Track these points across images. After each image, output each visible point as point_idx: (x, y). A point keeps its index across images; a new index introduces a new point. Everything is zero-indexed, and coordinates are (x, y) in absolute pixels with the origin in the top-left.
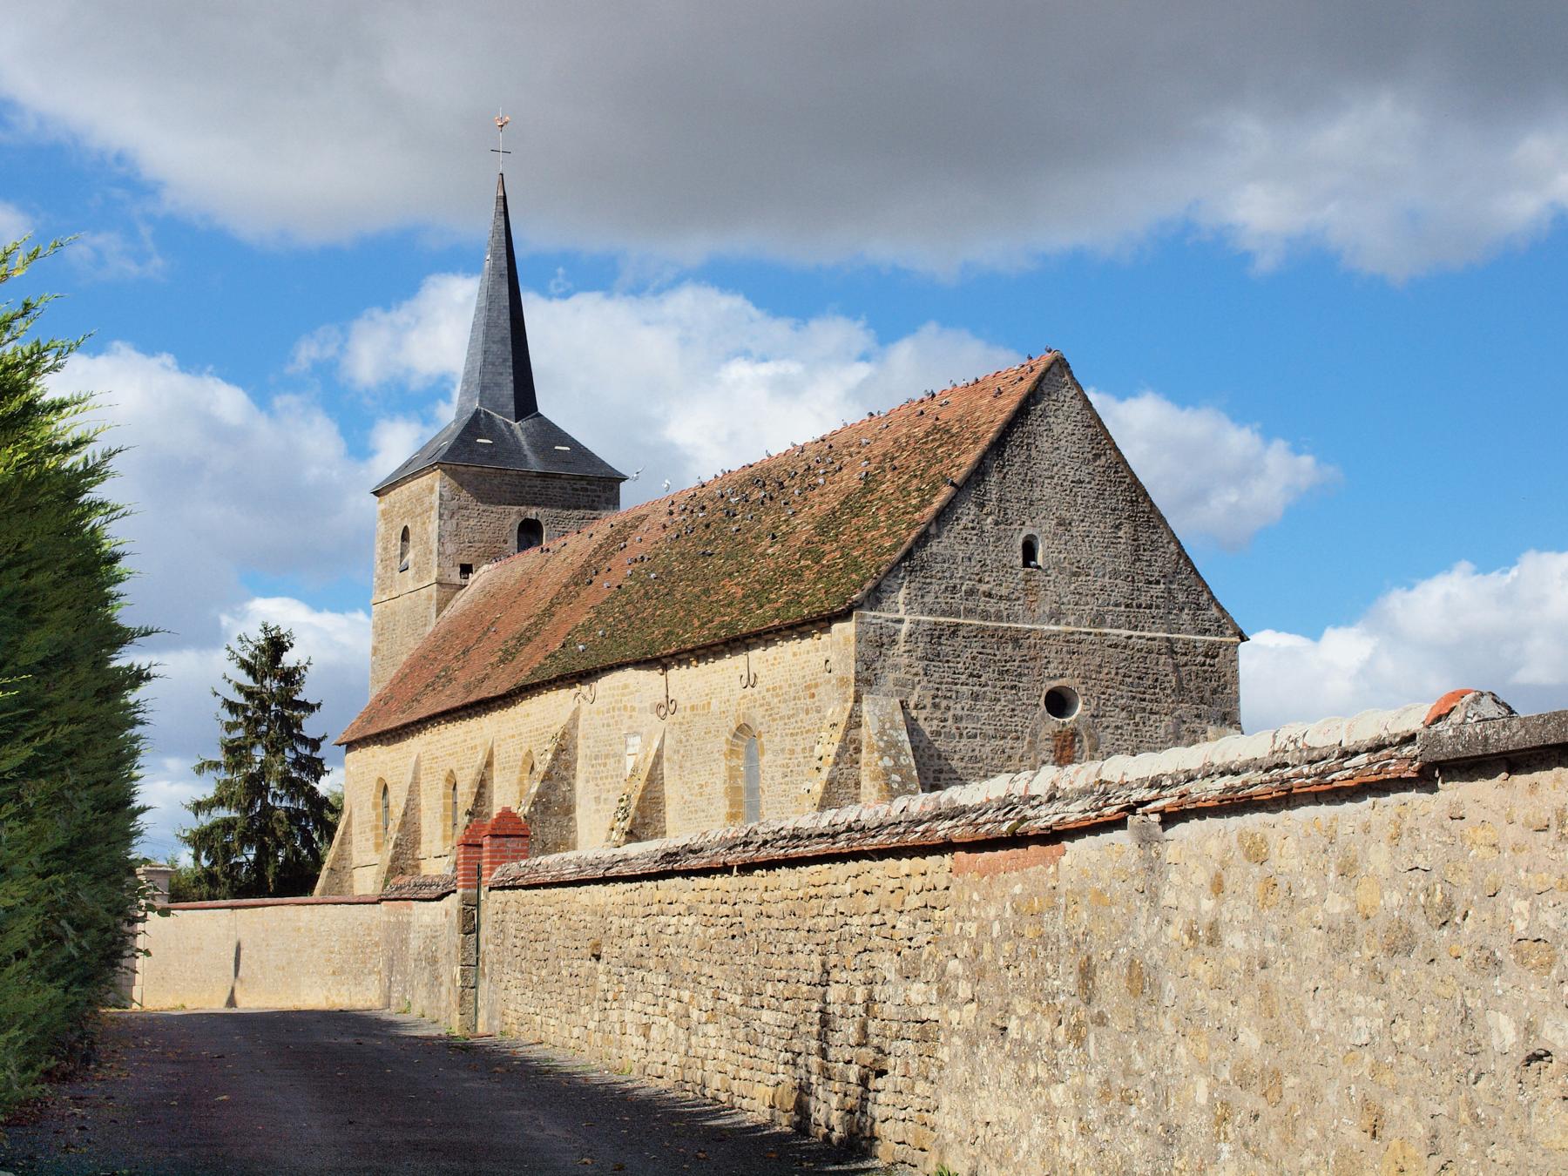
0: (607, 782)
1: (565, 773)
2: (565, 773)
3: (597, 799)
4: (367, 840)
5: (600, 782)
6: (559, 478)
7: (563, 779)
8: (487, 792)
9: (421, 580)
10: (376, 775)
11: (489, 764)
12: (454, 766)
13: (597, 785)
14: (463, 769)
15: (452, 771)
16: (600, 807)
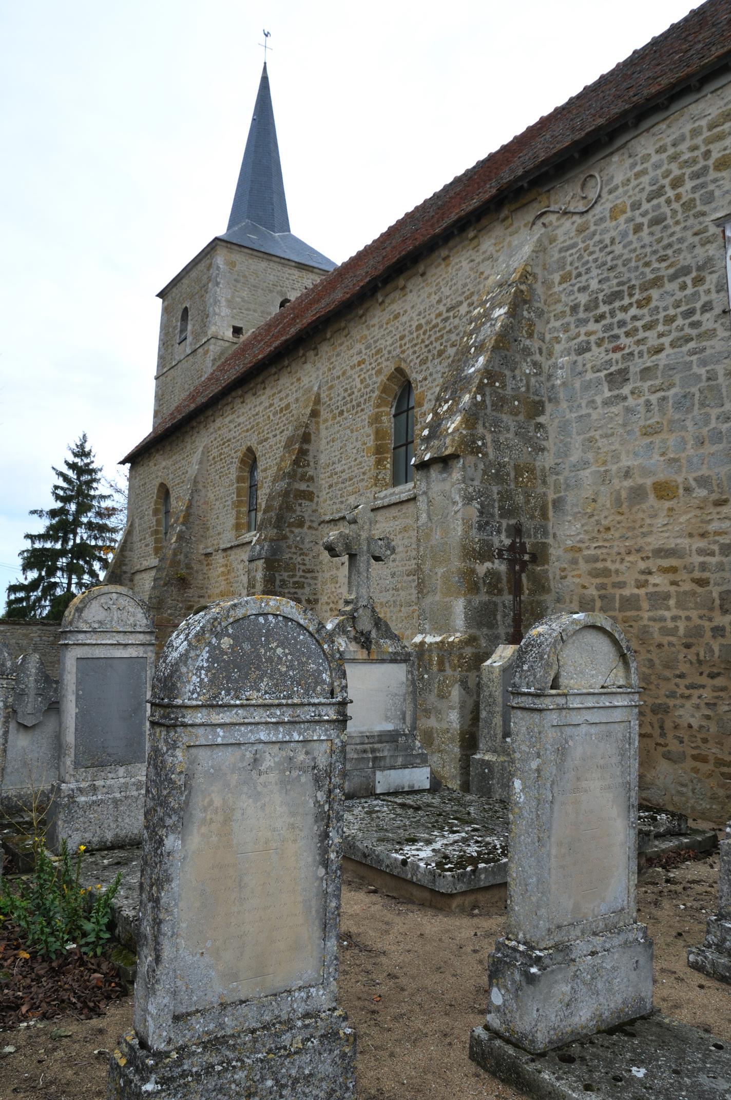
0: (651, 334)
1: (528, 342)
2: (528, 342)
3: (618, 378)
4: (147, 545)
5: (624, 341)
6: (312, 272)
7: (527, 352)
8: (312, 447)
9: (198, 341)
10: (157, 482)
11: (315, 414)
12: (253, 441)
13: (616, 349)
14: (266, 440)
15: (250, 450)
16: (626, 390)
